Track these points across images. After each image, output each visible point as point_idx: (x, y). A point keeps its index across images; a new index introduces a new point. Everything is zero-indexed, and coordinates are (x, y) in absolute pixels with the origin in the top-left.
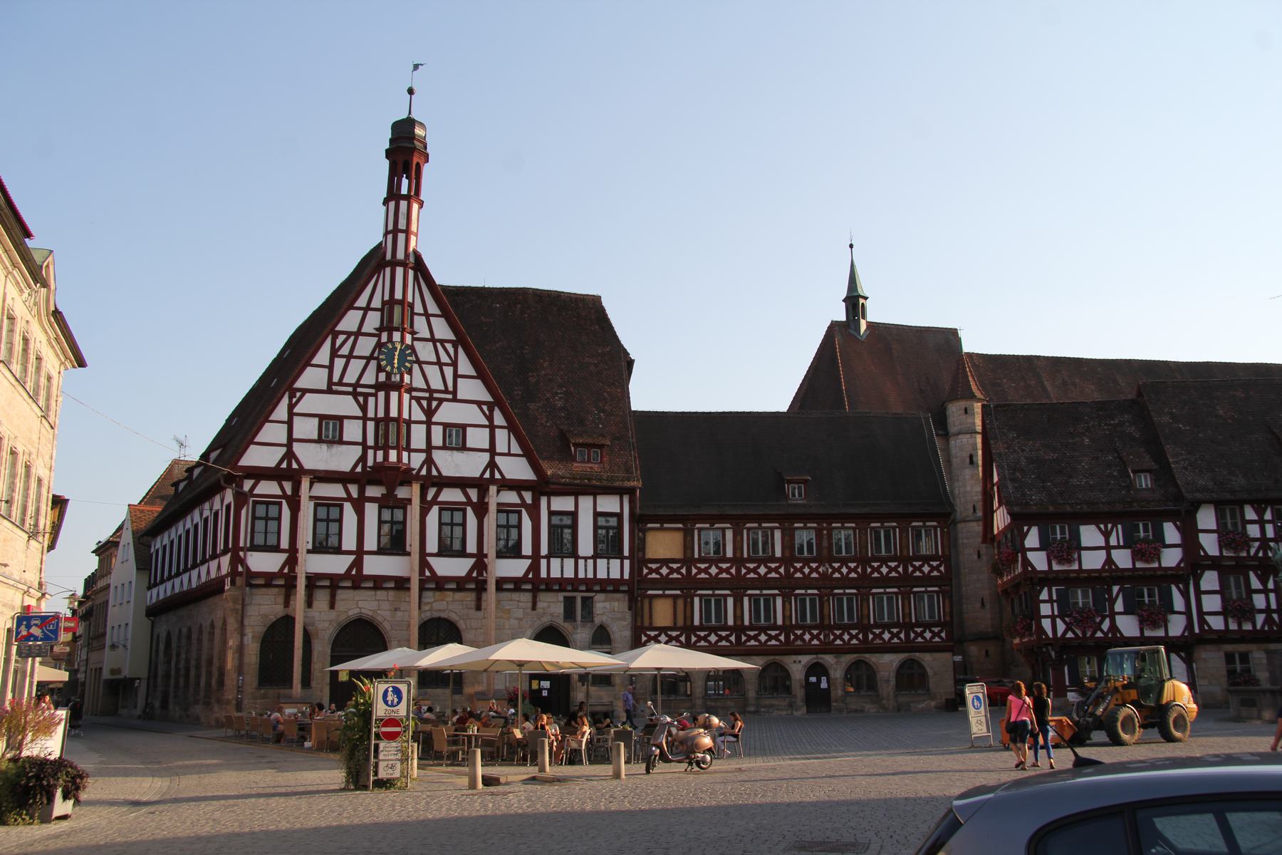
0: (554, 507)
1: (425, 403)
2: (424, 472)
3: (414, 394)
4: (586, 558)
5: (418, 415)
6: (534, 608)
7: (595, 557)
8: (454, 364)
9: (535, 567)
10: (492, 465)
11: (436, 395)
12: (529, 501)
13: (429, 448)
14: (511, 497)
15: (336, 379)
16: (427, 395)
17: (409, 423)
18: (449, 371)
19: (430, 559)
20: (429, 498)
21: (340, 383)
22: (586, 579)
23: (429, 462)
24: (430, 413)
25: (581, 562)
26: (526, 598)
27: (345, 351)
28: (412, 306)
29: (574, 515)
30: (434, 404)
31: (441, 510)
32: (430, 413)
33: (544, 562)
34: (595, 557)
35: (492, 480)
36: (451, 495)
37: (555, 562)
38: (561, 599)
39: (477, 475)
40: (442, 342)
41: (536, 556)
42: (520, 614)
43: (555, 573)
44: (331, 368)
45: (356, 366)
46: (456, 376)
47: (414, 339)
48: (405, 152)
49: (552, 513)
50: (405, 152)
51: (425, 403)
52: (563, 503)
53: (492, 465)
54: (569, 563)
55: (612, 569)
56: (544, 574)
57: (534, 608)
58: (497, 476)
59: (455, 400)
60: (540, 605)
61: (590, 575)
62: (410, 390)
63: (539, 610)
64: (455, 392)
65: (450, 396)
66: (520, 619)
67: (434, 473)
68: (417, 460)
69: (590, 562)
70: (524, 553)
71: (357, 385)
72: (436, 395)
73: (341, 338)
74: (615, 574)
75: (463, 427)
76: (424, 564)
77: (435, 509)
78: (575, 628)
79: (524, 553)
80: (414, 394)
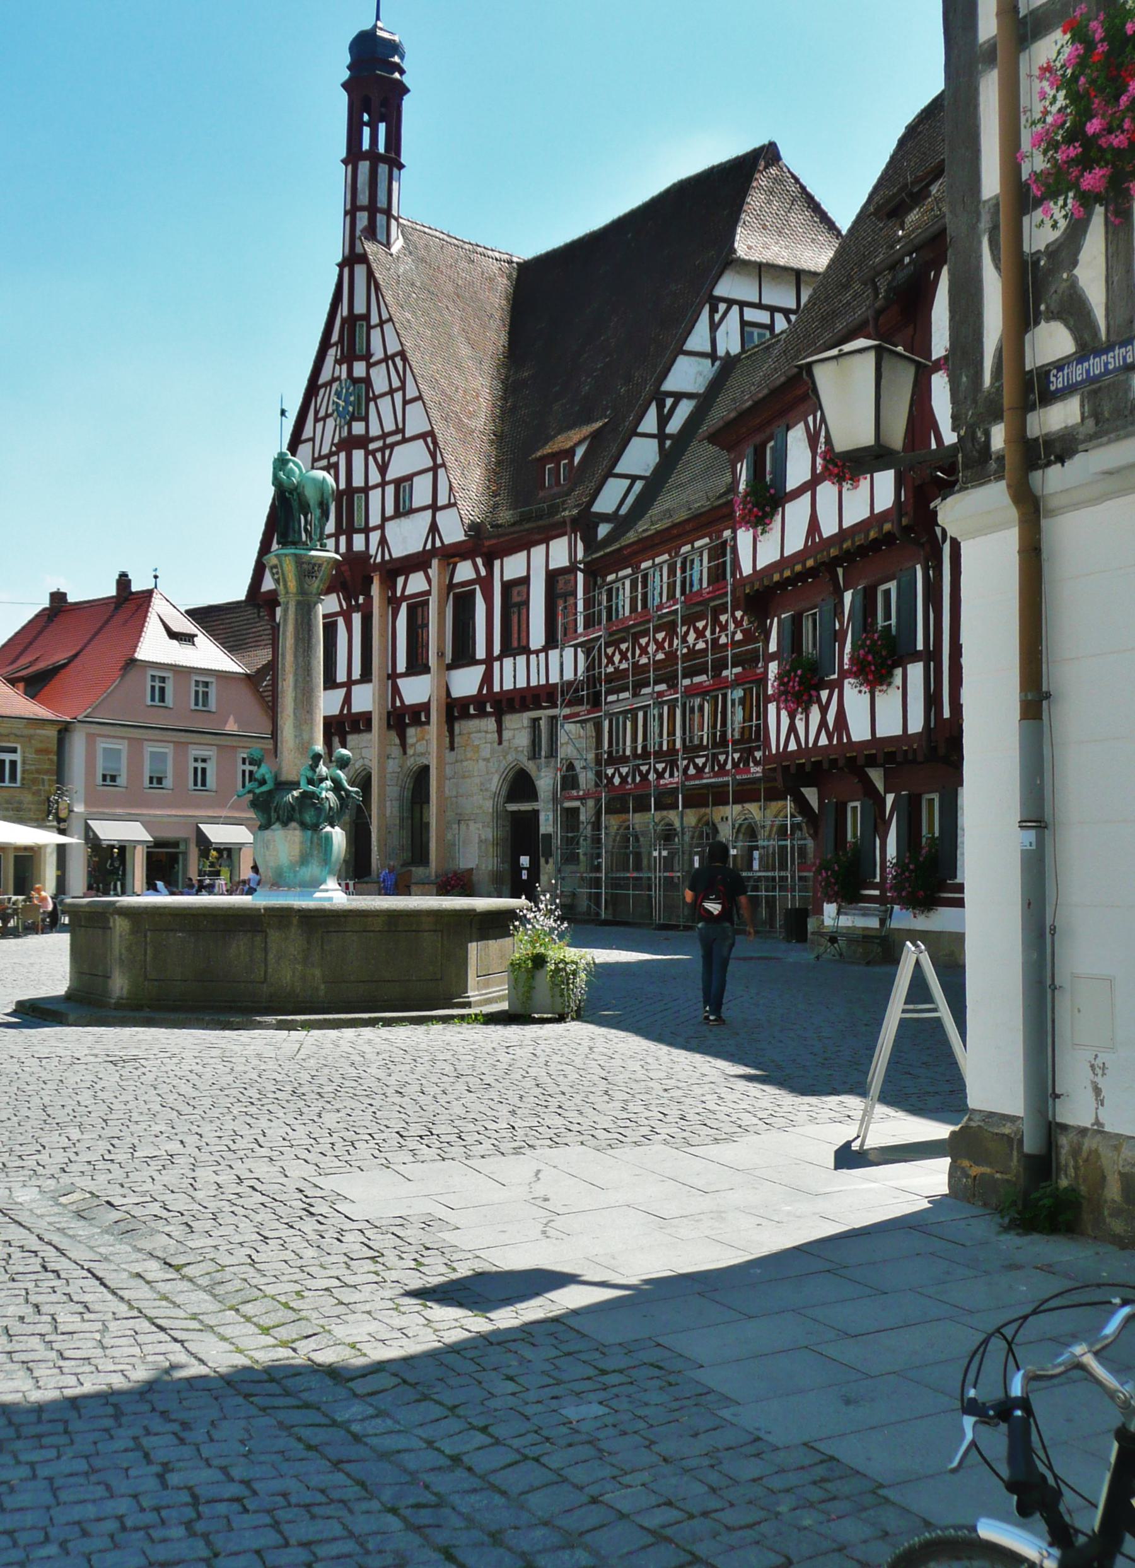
0: (505, 579)
1: (379, 456)
2: (379, 560)
3: (372, 446)
4: (537, 652)
5: (375, 477)
6: (500, 743)
7: (546, 649)
8: (403, 388)
9: (488, 678)
10: (434, 528)
11: (389, 440)
12: (483, 573)
13: (384, 519)
14: (465, 571)
15: (316, 455)
16: (379, 444)
17: (366, 489)
18: (398, 396)
19: (399, 681)
20: (398, 594)
21: (321, 458)
22: (539, 686)
23: (383, 542)
24: (383, 469)
25: (533, 657)
26: (490, 724)
27: (322, 414)
28: (367, 317)
29: (525, 581)
30: (387, 452)
31: (411, 610)
32: (383, 469)
33: (497, 665)
34: (546, 649)
35: (434, 552)
36: (416, 583)
37: (508, 662)
38: (526, 723)
39: (421, 549)
40: (393, 357)
41: (489, 661)
42: (486, 752)
43: (508, 685)
44: (313, 439)
45: (330, 422)
46: (405, 403)
47: (369, 366)
48: (375, 81)
49: (507, 586)
50: (375, 81)
51: (379, 456)
52: (513, 566)
53: (434, 528)
54: (521, 660)
55: (564, 665)
56: (497, 689)
57: (500, 743)
58: (438, 544)
59: (405, 440)
60: (506, 735)
61: (543, 682)
62: (363, 442)
63: (505, 743)
64: (403, 431)
65: (399, 437)
66: (487, 760)
67: (387, 557)
68: (375, 537)
69: (542, 655)
70: (478, 657)
71: (331, 454)
72: (389, 440)
73: (322, 391)
74: (569, 675)
75: (409, 478)
76: (396, 691)
77: (404, 606)
78: (539, 769)
79: (478, 657)
80: (372, 446)
